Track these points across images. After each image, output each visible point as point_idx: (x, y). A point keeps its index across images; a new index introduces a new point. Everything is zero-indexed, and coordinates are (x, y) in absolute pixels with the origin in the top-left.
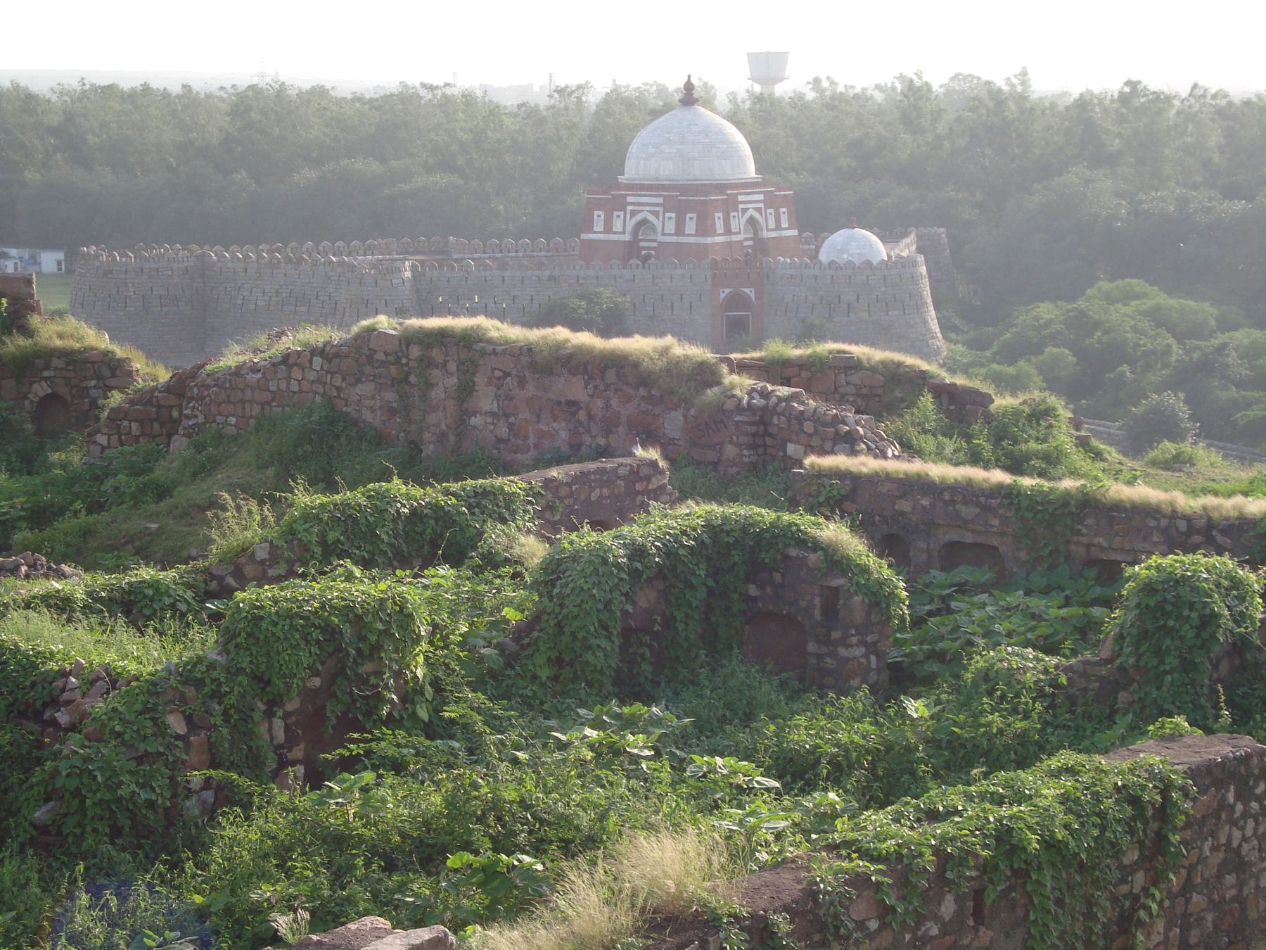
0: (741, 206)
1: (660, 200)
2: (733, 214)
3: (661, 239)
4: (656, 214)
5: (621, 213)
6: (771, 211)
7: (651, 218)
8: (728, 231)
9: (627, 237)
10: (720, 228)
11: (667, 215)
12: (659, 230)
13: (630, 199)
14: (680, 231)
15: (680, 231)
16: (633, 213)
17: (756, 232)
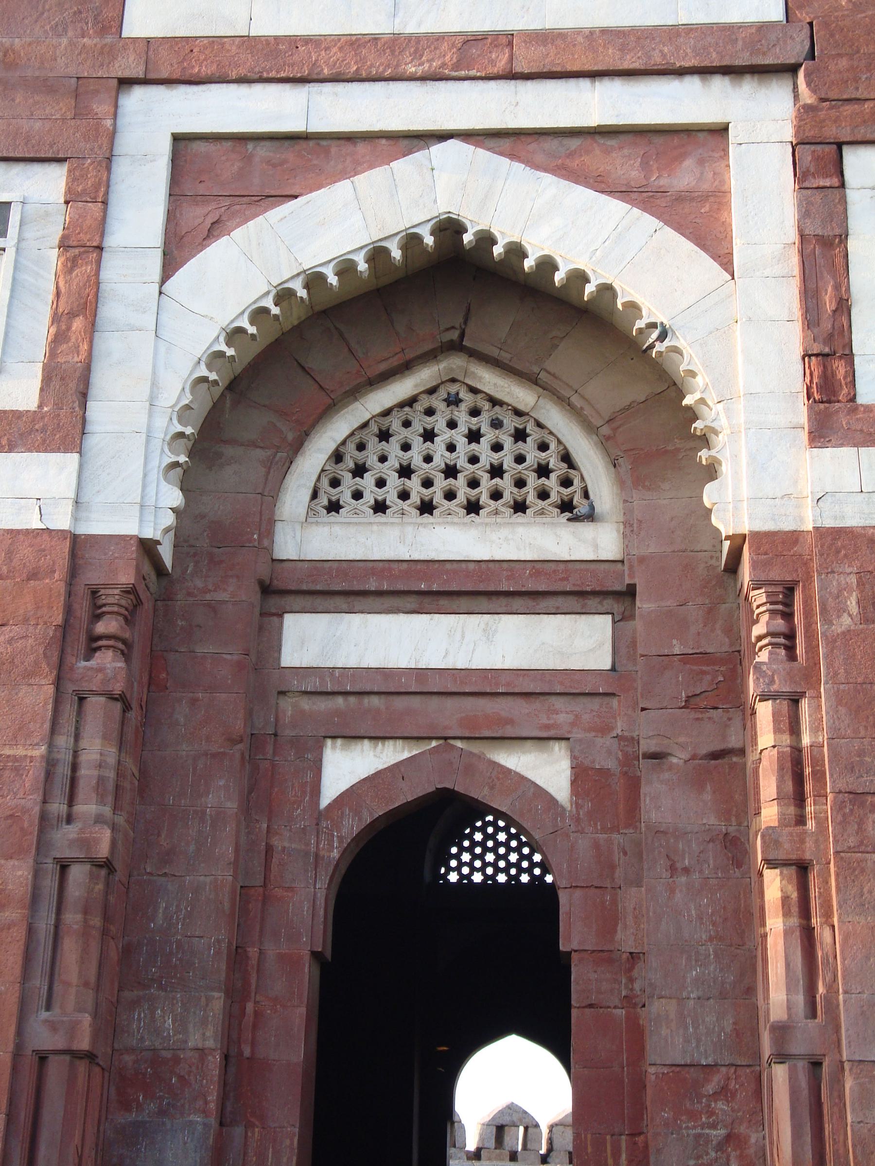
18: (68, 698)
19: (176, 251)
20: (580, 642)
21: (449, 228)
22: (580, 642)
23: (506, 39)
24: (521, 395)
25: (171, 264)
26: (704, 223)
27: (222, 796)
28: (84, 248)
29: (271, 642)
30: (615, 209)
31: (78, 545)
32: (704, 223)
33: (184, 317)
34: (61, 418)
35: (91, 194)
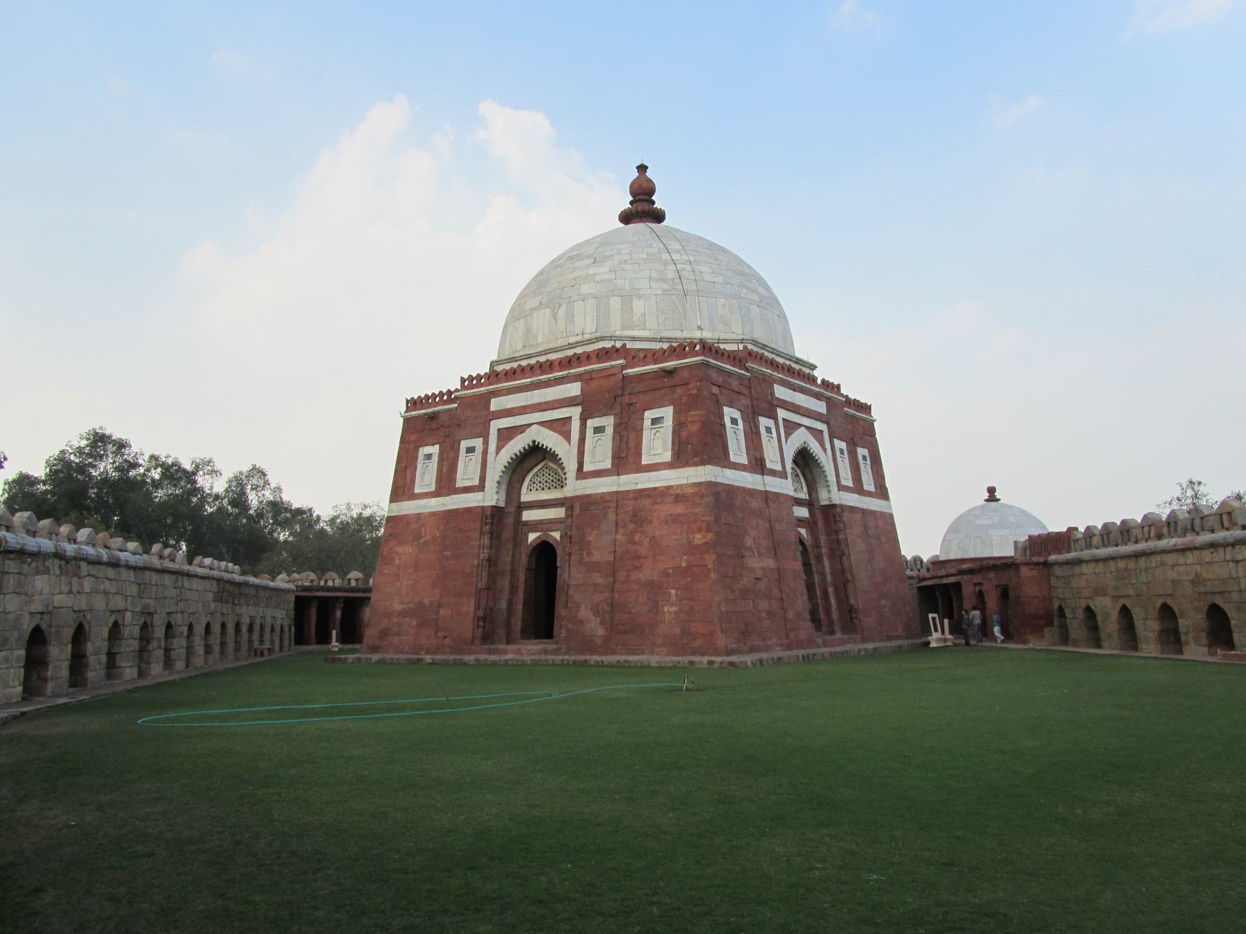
0: (782, 414)
1: (574, 389)
2: (764, 422)
3: (574, 487)
4: (561, 426)
5: (478, 443)
6: (840, 444)
7: (550, 440)
8: (758, 465)
9: (491, 497)
10: (738, 451)
11: (592, 423)
12: (571, 466)
13: (496, 404)
14: (626, 456)
15: (626, 456)
16: (506, 435)
17: (812, 488)
18: (482, 533)
19: (498, 450)
20: (559, 513)
21: (534, 442)
22: (559, 513)
23: (540, 404)
24: (555, 467)
25: (497, 453)
26: (567, 437)
27: (510, 546)
28: (485, 453)
29: (519, 514)
30: (556, 435)
31: (483, 508)
32: (567, 437)
33: (500, 461)
34: (481, 487)
35: (486, 443)
